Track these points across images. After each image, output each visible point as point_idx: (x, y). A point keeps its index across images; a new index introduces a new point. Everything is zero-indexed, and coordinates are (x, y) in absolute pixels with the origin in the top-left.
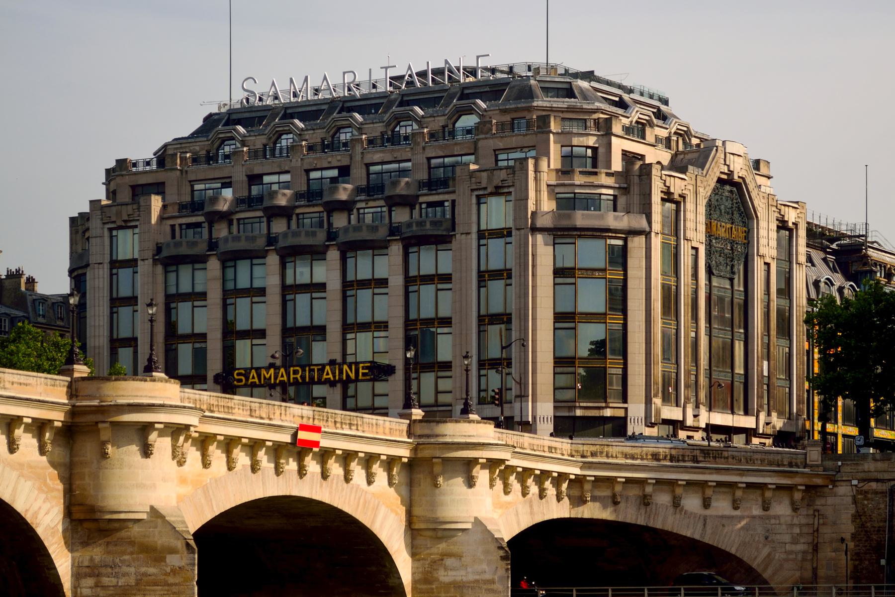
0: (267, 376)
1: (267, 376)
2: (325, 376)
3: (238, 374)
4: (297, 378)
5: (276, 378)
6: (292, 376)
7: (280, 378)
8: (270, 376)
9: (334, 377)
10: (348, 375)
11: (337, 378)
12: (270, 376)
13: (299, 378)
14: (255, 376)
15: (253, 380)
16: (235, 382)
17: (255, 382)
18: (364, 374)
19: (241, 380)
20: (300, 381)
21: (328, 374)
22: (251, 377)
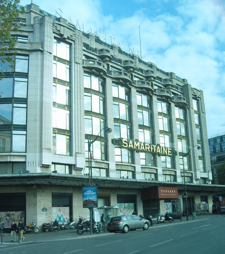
0: (137, 146)
1: (137, 146)
2: (158, 151)
3: (124, 142)
4: (147, 149)
5: (140, 148)
6: (146, 148)
7: (141, 148)
8: (138, 146)
9: (161, 152)
10: (165, 152)
11: (162, 153)
12: (138, 146)
13: (148, 149)
14: (132, 144)
15: (131, 146)
16: (123, 145)
17: (132, 147)
18: (170, 153)
19: (125, 145)
20: (149, 151)
21: (158, 150)
22: (130, 144)
